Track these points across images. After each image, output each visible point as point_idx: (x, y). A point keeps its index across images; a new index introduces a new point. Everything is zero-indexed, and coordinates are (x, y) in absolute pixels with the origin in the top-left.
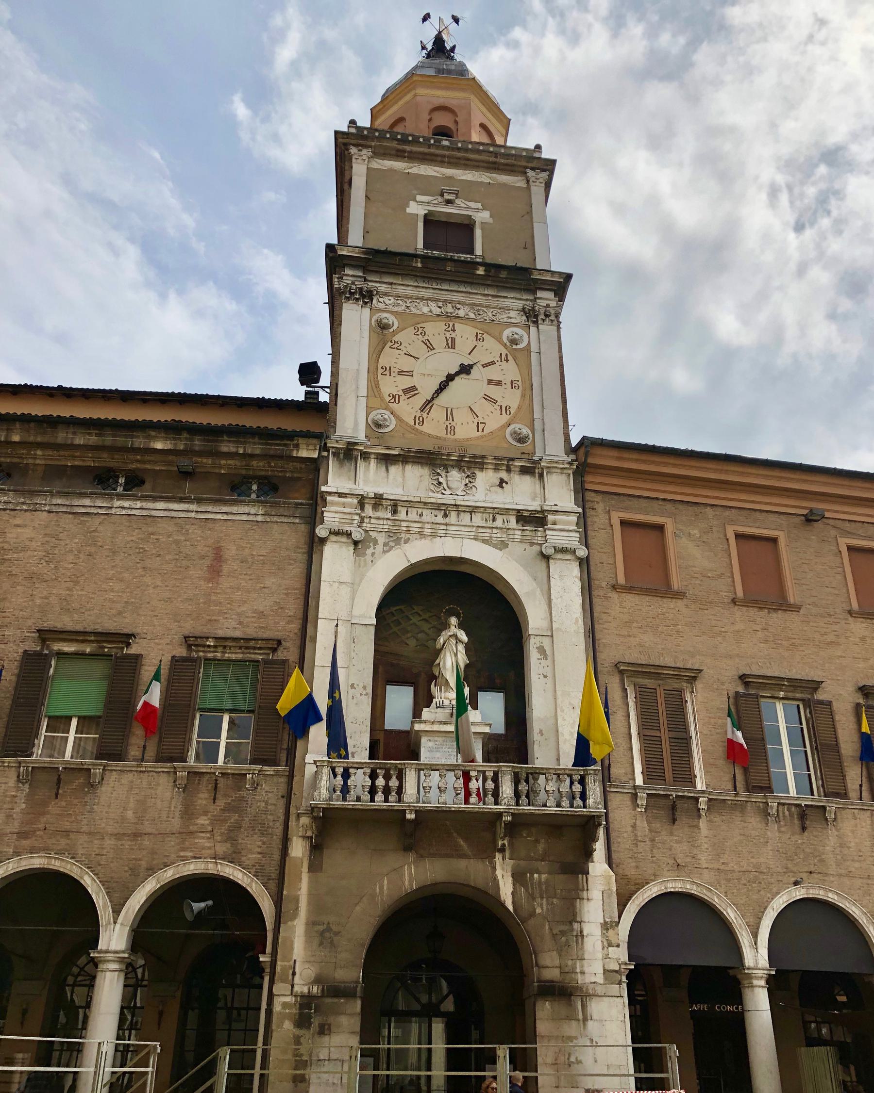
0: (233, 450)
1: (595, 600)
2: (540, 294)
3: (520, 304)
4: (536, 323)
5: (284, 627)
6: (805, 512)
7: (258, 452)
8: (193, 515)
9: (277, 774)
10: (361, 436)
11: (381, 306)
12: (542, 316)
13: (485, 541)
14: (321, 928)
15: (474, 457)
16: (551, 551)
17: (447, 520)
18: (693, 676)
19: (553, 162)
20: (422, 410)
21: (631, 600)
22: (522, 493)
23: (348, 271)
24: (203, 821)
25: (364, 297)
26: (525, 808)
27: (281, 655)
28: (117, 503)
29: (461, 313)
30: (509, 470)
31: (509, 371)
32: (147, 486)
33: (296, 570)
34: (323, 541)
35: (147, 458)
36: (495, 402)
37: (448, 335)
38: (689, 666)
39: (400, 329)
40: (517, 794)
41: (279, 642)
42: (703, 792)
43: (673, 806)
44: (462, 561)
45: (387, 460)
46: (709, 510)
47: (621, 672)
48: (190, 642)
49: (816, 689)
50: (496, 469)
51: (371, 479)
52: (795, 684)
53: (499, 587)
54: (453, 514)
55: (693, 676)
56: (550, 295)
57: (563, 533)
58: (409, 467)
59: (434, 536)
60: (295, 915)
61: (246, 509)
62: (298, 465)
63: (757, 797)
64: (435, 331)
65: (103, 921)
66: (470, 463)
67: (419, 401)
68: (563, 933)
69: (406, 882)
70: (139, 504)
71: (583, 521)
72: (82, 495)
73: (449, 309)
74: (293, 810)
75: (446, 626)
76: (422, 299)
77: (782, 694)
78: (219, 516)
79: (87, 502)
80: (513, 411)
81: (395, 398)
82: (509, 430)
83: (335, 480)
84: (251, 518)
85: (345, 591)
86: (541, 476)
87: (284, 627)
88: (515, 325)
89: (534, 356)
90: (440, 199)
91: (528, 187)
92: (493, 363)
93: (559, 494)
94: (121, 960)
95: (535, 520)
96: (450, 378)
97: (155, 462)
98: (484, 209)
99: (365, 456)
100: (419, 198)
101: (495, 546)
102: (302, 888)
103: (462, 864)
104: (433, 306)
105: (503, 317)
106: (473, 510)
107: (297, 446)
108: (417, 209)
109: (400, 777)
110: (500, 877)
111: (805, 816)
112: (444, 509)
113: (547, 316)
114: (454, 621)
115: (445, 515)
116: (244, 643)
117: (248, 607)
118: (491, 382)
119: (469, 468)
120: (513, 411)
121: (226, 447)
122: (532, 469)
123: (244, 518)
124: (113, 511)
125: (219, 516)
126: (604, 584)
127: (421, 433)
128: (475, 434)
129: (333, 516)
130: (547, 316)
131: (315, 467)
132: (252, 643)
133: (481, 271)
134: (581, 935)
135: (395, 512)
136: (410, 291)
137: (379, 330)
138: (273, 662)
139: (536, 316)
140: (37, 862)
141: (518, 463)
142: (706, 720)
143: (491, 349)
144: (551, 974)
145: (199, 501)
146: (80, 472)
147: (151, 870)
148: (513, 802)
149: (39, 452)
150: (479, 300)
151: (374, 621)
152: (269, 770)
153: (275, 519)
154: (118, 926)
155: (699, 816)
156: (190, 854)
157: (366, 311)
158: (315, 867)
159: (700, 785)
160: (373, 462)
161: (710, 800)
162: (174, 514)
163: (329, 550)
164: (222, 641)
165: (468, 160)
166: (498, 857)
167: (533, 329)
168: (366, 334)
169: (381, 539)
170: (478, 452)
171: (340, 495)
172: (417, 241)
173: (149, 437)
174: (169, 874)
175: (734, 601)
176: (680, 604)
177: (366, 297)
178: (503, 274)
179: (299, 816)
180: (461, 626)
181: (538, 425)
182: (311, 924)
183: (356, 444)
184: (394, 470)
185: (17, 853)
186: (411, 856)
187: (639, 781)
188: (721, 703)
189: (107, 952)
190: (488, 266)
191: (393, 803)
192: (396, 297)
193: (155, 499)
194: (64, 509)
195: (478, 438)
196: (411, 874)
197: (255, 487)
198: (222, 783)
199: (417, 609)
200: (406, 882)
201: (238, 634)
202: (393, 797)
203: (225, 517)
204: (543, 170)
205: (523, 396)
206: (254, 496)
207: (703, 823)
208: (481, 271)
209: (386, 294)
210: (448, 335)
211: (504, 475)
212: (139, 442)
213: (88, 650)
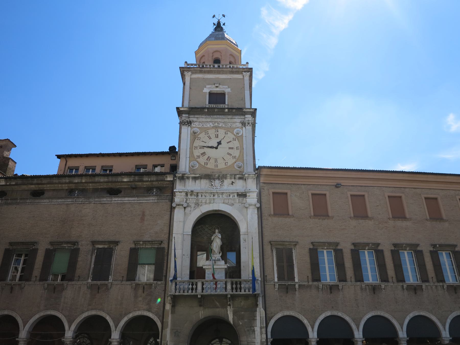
0: (147, 180)
1: (263, 221)
2: (247, 116)
3: (239, 120)
4: (245, 126)
5: (164, 237)
6: (336, 184)
7: (155, 180)
8: (136, 201)
9: (162, 284)
10: (187, 170)
11: (194, 126)
12: (247, 124)
13: (226, 204)
14: (175, 331)
15: (223, 175)
16: (247, 206)
17: (214, 197)
18: (296, 244)
19: (252, 69)
20: (207, 160)
21: (276, 219)
22: (239, 186)
23: (184, 115)
24: (140, 299)
25: (188, 123)
26: (234, 292)
27: (162, 246)
28: (114, 199)
29: (220, 125)
30: (235, 178)
31: (236, 144)
32: (123, 193)
33: (167, 217)
34: (174, 208)
35: (122, 184)
36: (231, 155)
37: (216, 133)
38: (294, 240)
39: (201, 133)
40: (232, 289)
41: (162, 242)
42: (297, 282)
43: (287, 288)
44: (219, 210)
45: (195, 178)
46: (303, 186)
47: (271, 244)
48: (136, 243)
49: (337, 245)
50: (231, 178)
51: (191, 185)
52: (330, 244)
53: (232, 218)
54: (216, 195)
55: (296, 244)
56: (250, 116)
57: (252, 199)
58: (202, 180)
59: (210, 203)
60: (167, 327)
61: (152, 198)
62: (167, 182)
63: (316, 283)
64: (212, 132)
65: (112, 330)
66: (222, 177)
67: (206, 157)
68: (248, 330)
69: (200, 317)
70: (120, 199)
72: (104, 197)
73: (216, 124)
74: (166, 295)
75: (214, 233)
76: (208, 122)
77: (326, 248)
78: (144, 201)
79: (105, 199)
80: (237, 157)
81: (199, 157)
82: (235, 164)
83: (179, 187)
84: (153, 201)
85: (182, 224)
86: (245, 179)
87: (164, 237)
88: (238, 127)
89: (244, 138)
90: (214, 86)
91: (243, 78)
92: (231, 141)
93: (251, 186)
94: (118, 342)
95: (243, 195)
97: (124, 185)
98: (228, 88)
99: (188, 178)
100: (207, 86)
101: (230, 205)
102: (169, 319)
103: (217, 310)
104: (211, 124)
105: (234, 126)
106: (222, 193)
107: (167, 177)
108: (206, 90)
109: (196, 285)
110: (229, 313)
111: (332, 288)
113: (248, 124)
114: (217, 231)
115: (214, 196)
116: (151, 242)
117: (152, 231)
118: (230, 148)
119: (222, 179)
120: (237, 157)
121: (145, 178)
123: (151, 201)
124: (112, 202)
125: (144, 201)
126: (266, 215)
127: (207, 168)
128: (224, 166)
129: (177, 199)
130: (248, 124)
131: (173, 183)
132: (154, 242)
133: (226, 110)
134: (254, 331)
135: (197, 196)
136: (204, 120)
137: (193, 134)
138: (160, 248)
139: (245, 124)
140: (93, 313)
141: (238, 176)
145: (138, 196)
146: (103, 190)
147: (126, 314)
148: (231, 291)
149: (91, 185)
150: (226, 120)
151: (190, 233)
152: (159, 282)
153: (161, 201)
154: (116, 332)
155: (296, 290)
156: (136, 309)
157: (189, 128)
158: (173, 312)
159: (296, 280)
160: (191, 179)
161: (299, 285)
162: (130, 201)
163: (176, 211)
164: (145, 242)
165: (223, 71)
166: (229, 307)
167: (244, 128)
168: (189, 136)
169: (193, 205)
170: (224, 173)
171: (180, 192)
172: (206, 102)
173: (122, 178)
174: (131, 316)
175: (310, 217)
177: (189, 123)
178: (234, 111)
179: (168, 297)
180: (219, 232)
181: (245, 162)
182: (172, 330)
183: (185, 174)
184: (198, 182)
185: (88, 310)
186: (202, 308)
187: (276, 280)
188: (306, 252)
189: (114, 339)
191: (194, 293)
192: (200, 122)
193: (125, 197)
194: (98, 202)
195: (225, 168)
196: (202, 313)
197: (155, 190)
198: (146, 287)
199: (207, 226)
200: (200, 317)
201: (150, 239)
202: (194, 291)
203: (146, 201)
204: (249, 72)
205: (240, 152)
206: (154, 193)
207: (297, 293)
208: (226, 110)
209: (196, 122)
210: (216, 133)
211: (233, 180)
212: (119, 179)
213: (106, 247)
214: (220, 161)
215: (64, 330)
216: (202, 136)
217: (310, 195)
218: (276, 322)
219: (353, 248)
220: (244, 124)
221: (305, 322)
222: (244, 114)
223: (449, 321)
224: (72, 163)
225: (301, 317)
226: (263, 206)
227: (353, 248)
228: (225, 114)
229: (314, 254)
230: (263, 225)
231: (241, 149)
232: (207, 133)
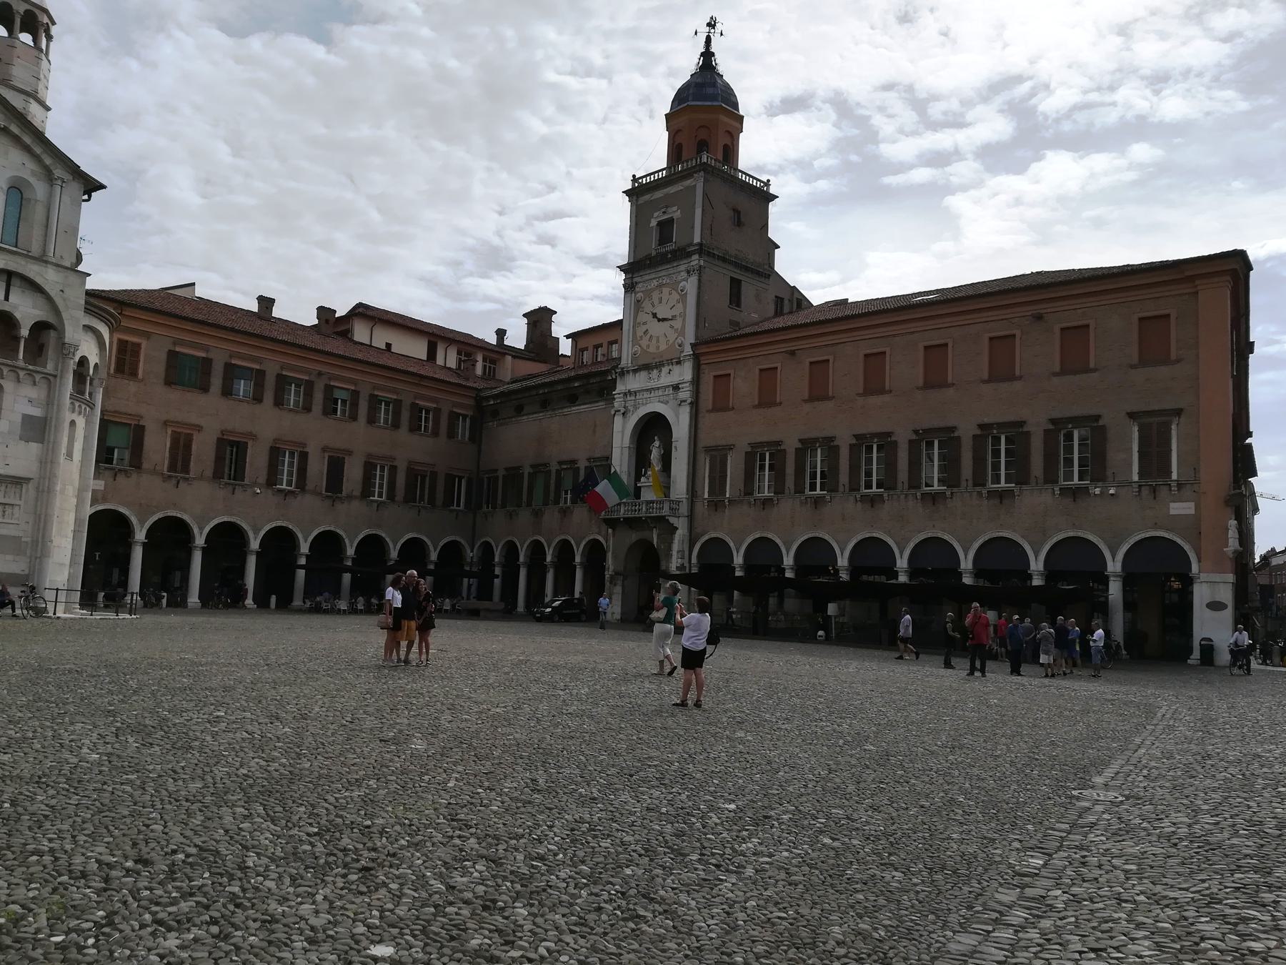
45: (635, 371)
52: (769, 444)
55: (730, 448)
56: (696, 257)
57: (685, 394)
66: (659, 366)
71: (696, 381)
83: (620, 387)
95: (676, 388)
96: (659, 320)
108: (654, 223)
111: (766, 503)
112: (650, 390)
122: (679, 363)
129: (618, 403)
131: (614, 381)
136: (647, 277)
142: (734, 466)
143: (676, 296)
144: (663, 568)
150: (671, 271)
176: (731, 413)
187: (706, 496)
190: (673, 252)
196: (634, 537)
214: (662, 340)
215: (545, 554)
216: (647, 306)
217: (757, 372)
218: (703, 545)
219: (800, 446)
220: (688, 272)
221: (732, 545)
222: (689, 255)
223: (912, 545)
225: (728, 540)
226: (702, 397)
227: (800, 446)
228: (669, 261)
229: (750, 457)
230: (700, 425)
231: (683, 315)
232: (650, 298)
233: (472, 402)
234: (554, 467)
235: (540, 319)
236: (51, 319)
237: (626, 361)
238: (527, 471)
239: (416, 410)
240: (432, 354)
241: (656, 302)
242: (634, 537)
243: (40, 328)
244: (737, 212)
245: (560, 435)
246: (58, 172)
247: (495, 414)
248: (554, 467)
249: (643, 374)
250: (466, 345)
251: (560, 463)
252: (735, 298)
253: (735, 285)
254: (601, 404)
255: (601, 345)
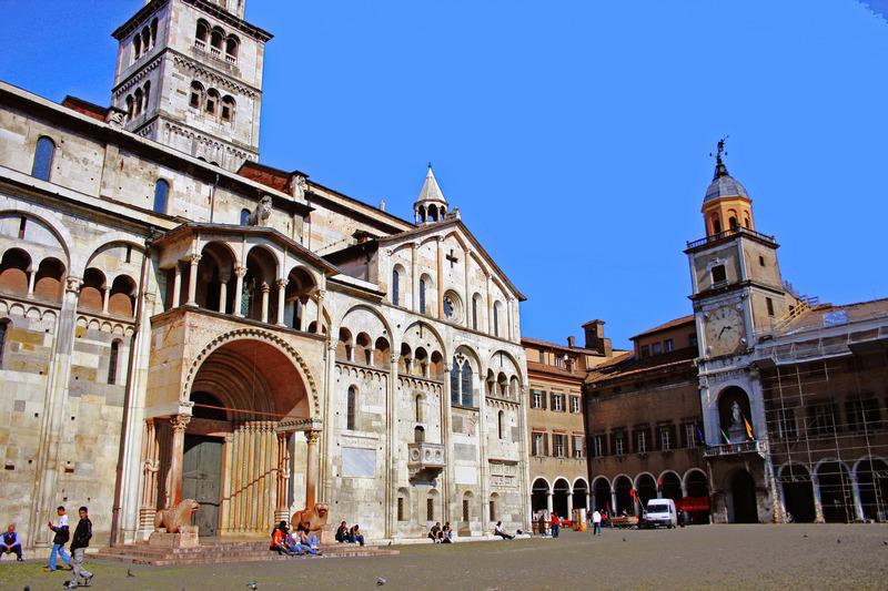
64: (719, 313)
83: (701, 372)
131: (696, 370)
158: (712, 467)
196: (731, 467)
222: (742, 287)
224: (643, 343)
228: (726, 291)
233: (579, 388)
234: (653, 426)
235: (591, 329)
236: (516, 374)
237: (703, 354)
238: (630, 429)
239: (553, 396)
240: (542, 358)
241: (720, 317)
242: (731, 467)
243: (513, 377)
244: (761, 259)
245: (660, 403)
246: (511, 295)
247: (596, 394)
248: (653, 426)
249: (719, 362)
250: (559, 353)
251: (658, 423)
252: (771, 312)
253: (769, 300)
254: (687, 383)
255: (658, 343)
